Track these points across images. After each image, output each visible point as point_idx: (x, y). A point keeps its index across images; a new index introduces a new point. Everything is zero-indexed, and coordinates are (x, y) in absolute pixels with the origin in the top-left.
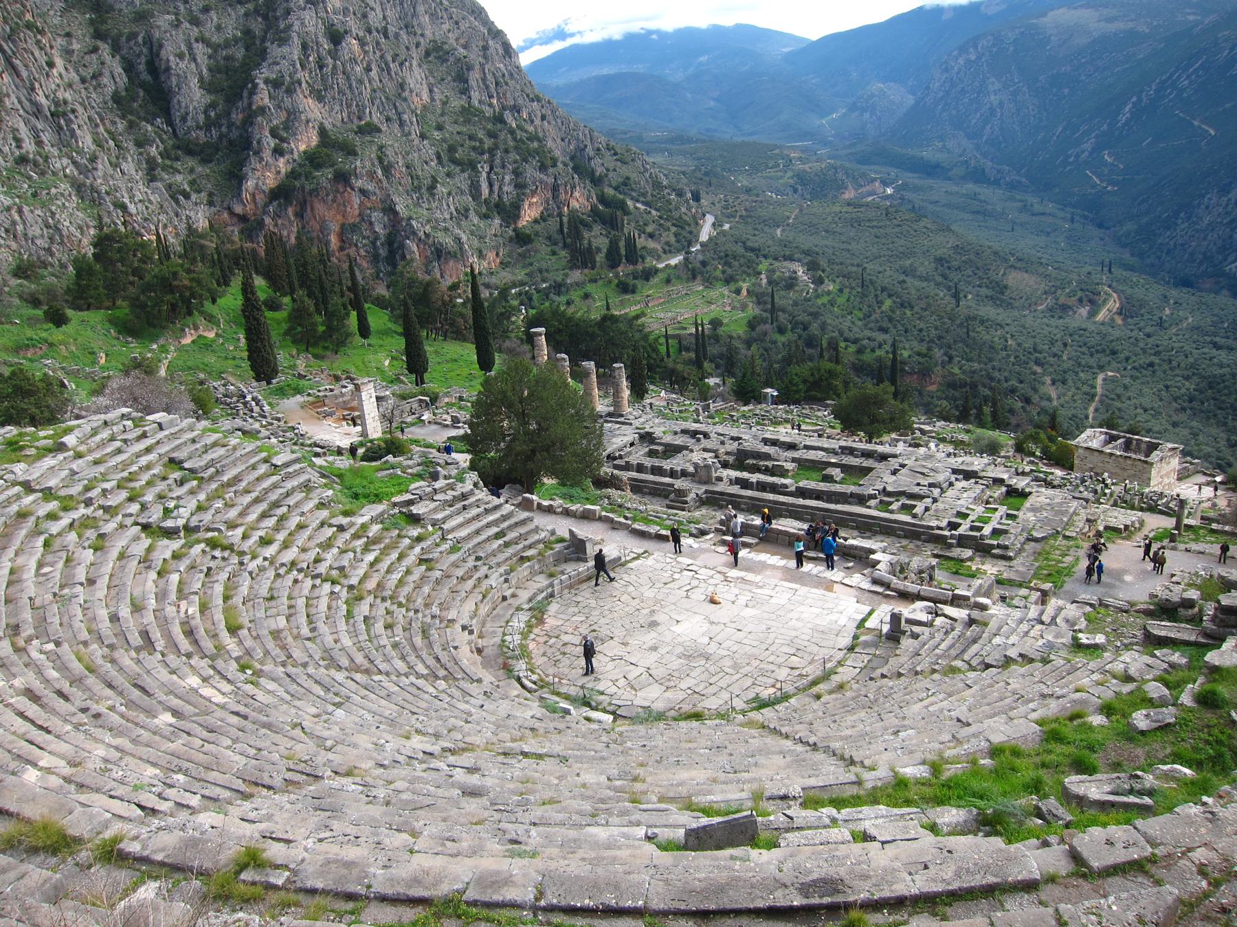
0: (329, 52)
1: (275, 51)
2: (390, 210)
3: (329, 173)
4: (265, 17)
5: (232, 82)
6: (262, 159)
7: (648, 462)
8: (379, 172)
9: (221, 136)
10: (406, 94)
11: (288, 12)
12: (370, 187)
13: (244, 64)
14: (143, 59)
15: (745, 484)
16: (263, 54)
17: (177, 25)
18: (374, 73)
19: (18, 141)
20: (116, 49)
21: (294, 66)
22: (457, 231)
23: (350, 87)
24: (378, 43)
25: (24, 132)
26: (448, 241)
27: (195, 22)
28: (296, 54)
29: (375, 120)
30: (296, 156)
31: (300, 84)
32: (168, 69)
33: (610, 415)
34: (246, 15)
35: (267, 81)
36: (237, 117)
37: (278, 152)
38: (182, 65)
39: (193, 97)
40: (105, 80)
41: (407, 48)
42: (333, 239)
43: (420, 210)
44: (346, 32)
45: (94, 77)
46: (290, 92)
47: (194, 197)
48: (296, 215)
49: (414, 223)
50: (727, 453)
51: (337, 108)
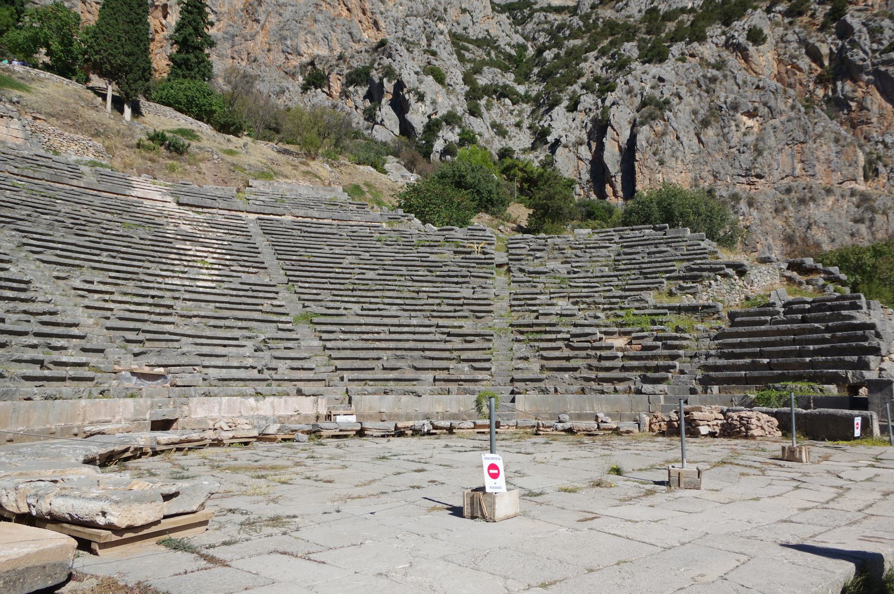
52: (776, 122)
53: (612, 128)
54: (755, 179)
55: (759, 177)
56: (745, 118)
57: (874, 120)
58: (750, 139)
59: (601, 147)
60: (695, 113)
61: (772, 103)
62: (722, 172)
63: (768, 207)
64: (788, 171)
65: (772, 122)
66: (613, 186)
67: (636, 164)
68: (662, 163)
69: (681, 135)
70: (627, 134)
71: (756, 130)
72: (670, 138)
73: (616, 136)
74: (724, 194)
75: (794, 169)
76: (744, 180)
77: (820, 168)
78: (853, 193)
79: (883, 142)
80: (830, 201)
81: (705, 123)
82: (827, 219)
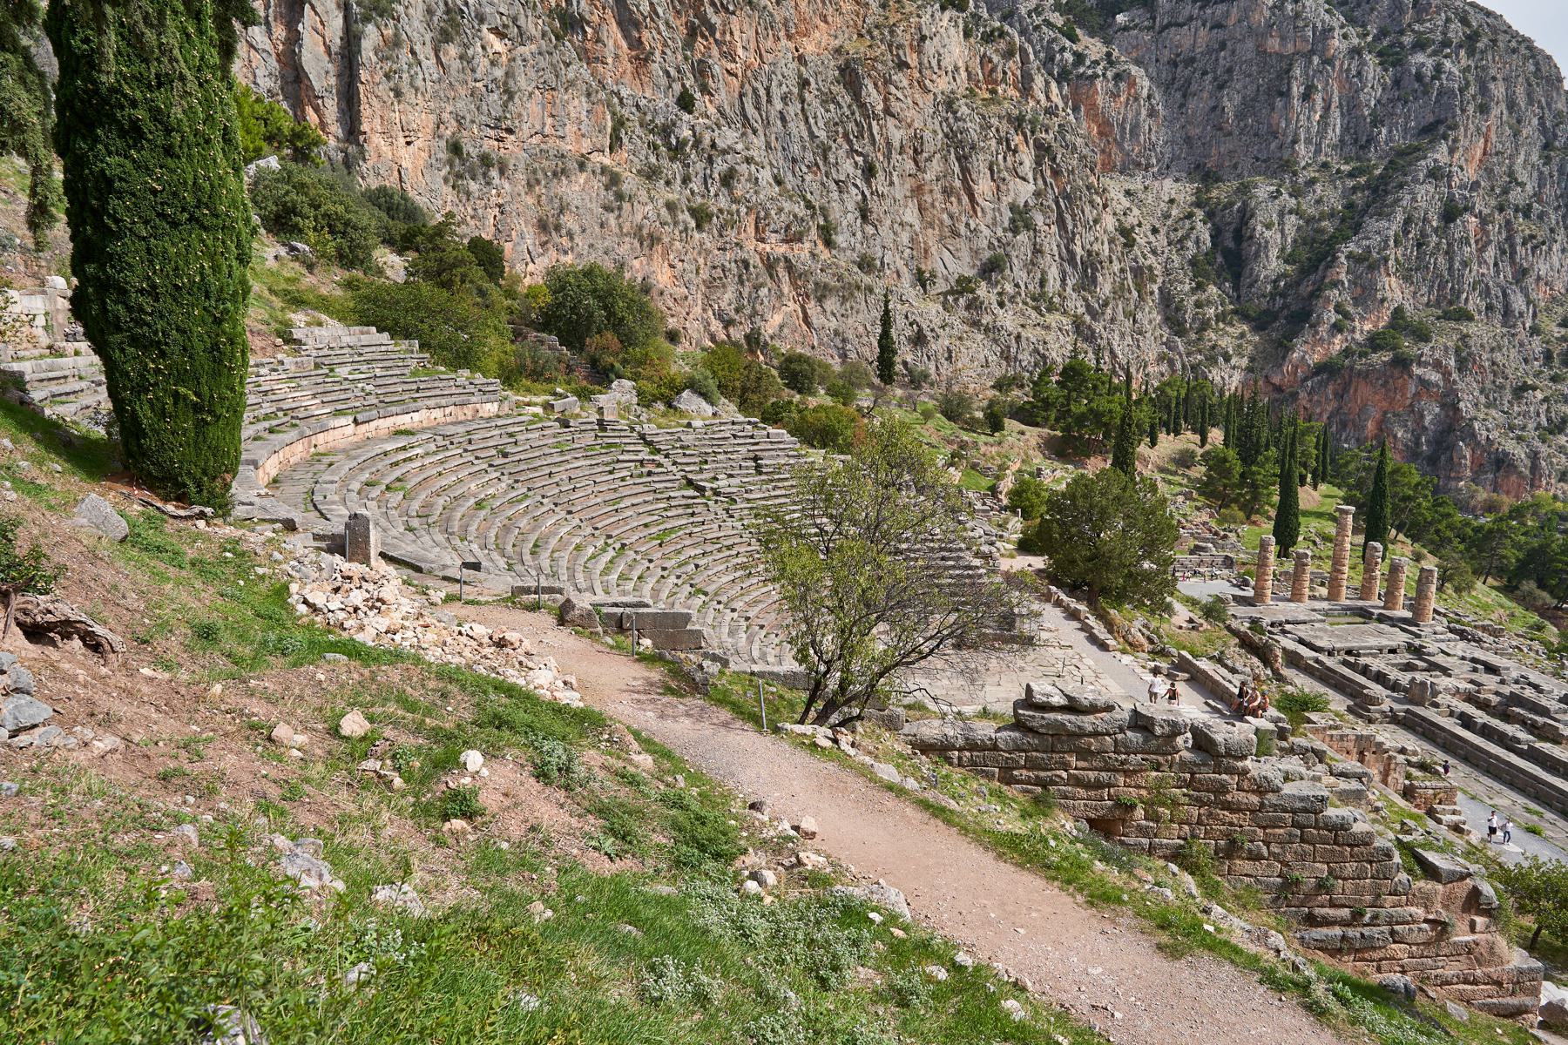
0: (1436, 230)
1: (1372, 224)
2: (1450, 403)
3: (1386, 357)
4: (1375, 191)
5: (1314, 255)
6: (1317, 332)
7: (1377, 664)
8: (1452, 363)
9: (1285, 306)
10: (1530, 281)
11: (1401, 186)
12: (1435, 377)
13: (1332, 237)
14: (1232, 227)
15: (1466, 721)
16: (1357, 228)
17: (1275, 196)
18: (1490, 254)
19: (1043, 283)
20: (1210, 216)
21: (1386, 242)
22: (1537, 443)
23: (1450, 269)
24: (1508, 222)
25: (1053, 273)
26: (1519, 452)
27: (1295, 193)
28: (1394, 227)
29: (1471, 307)
30: (1357, 336)
31: (1386, 260)
32: (1251, 237)
33: (1405, 620)
34: (1354, 189)
35: (1349, 256)
36: (1306, 289)
37: (1337, 328)
38: (1267, 234)
39: (1272, 265)
40: (1190, 244)
41: (1552, 231)
42: (1370, 425)
43: (1493, 412)
44: (1466, 209)
45: (1180, 241)
46: (1373, 267)
47: (1233, 361)
48: (1335, 394)
49: (1476, 425)
50: (1497, 693)
51: (1424, 289)
52: (525, 50)
53: (313, 8)
54: (504, 135)
55: (510, 131)
56: (492, 37)
57: (610, 60)
58: (499, 73)
59: (294, 39)
60: (430, 12)
61: (522, 22)
62: (468, 117)
63: (521, 177)
64: (538, 127)
65: (521, 49)
66: (317, 110)
67: (361, 88)
68: (398, 94)
69: (417, 48)
70: (336, 23)
71: (504, 58)
72: (404, 56)
73: (320, 26)
74: (474, 152)
75: (544, 124)
76: (492, 133)
77: (570, 129)
78: (604, 170)
79: (618, 94)
80: (582, 178)
81: (445, 37)
82: (578, 203)
